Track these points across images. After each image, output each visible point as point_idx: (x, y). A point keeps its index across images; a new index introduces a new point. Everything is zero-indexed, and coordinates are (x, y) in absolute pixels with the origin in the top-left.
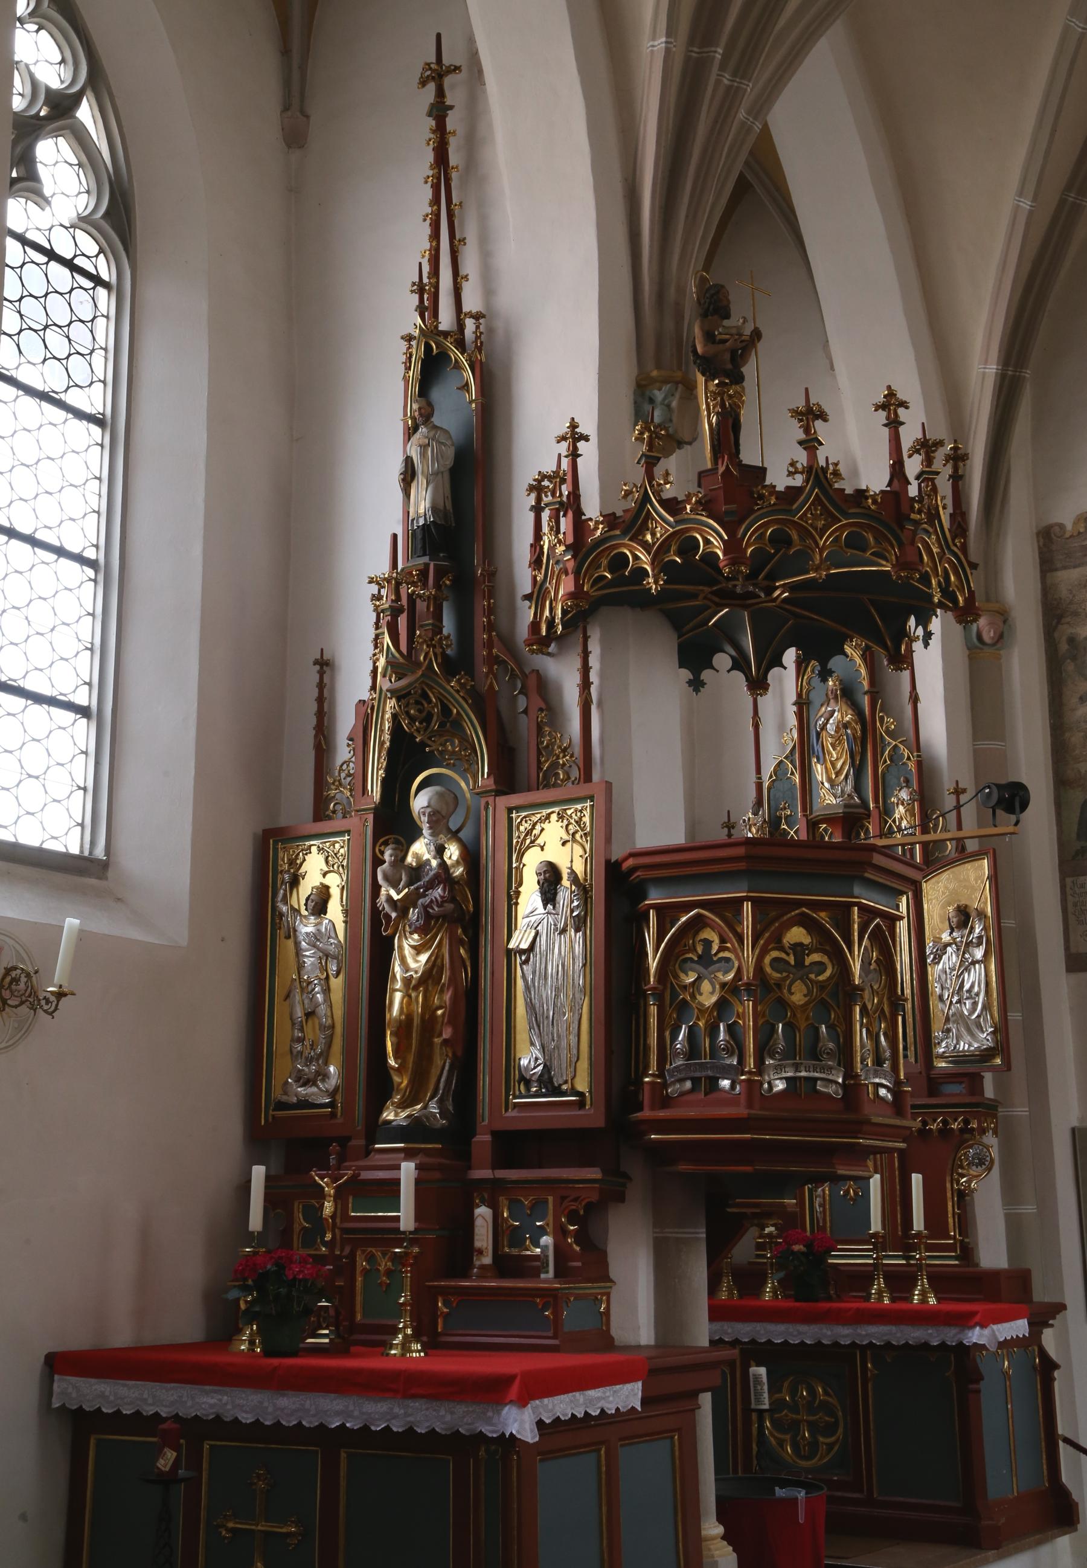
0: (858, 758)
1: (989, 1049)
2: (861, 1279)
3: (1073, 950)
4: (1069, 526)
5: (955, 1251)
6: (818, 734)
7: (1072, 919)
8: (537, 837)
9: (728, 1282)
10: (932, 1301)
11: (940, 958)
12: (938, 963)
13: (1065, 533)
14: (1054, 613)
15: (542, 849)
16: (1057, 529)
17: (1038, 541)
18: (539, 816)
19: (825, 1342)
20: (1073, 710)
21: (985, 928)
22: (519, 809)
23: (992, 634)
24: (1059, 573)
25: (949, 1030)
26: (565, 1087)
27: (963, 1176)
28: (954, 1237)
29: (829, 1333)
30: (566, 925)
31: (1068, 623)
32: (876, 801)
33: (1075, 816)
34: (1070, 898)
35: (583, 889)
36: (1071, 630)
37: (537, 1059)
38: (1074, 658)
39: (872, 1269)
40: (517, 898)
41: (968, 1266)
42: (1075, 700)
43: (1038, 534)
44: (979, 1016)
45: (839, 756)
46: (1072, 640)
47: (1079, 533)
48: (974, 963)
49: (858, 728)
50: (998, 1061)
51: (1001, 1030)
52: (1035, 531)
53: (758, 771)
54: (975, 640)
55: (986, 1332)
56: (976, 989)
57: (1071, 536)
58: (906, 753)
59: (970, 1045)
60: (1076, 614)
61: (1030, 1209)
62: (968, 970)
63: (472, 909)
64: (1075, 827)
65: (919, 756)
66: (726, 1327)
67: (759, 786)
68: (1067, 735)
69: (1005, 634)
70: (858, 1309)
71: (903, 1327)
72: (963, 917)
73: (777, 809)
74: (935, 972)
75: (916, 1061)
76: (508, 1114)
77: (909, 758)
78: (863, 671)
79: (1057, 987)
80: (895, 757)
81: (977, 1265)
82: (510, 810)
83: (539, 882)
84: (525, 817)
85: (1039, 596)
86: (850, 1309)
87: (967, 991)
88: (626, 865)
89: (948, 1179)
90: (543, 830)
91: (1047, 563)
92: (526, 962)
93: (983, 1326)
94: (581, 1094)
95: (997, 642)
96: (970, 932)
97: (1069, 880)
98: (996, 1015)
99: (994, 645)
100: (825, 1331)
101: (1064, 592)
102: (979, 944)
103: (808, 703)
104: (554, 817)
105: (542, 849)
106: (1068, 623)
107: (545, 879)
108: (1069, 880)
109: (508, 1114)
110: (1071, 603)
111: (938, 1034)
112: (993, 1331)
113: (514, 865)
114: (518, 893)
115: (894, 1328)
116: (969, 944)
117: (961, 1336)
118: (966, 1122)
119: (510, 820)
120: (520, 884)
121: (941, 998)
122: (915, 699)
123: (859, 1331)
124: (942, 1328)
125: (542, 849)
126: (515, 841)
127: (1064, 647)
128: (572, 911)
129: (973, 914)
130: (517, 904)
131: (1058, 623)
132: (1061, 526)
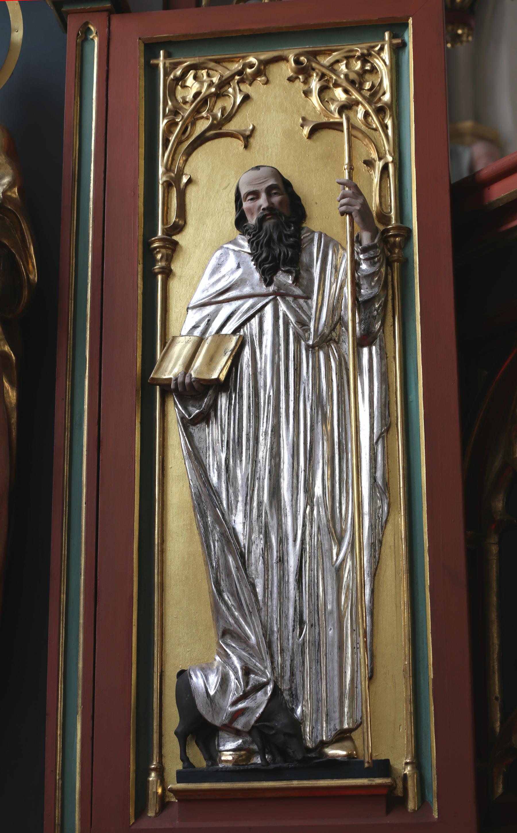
8: (228, 118)
15: (247, 139)
18: (236, 66)
22: (173, 46)
26: (336, 752)
30: (337, 322)
35: (384, 242)
37: (247, 671)
40: (169, 259)
63: (34, 277)
76: (143, 824)
82: (151, 49)
83: (241, 222)
84: (195, 67)
88: (500, 192)
90: (246, 98)
92: (206, 417)
94: (383, 767)
104: (287, 69)
105: (247, 139)
107: (271, 209)
109: (143, 824)
113: (162, 178)
114: (172, 248)
119: (151, 71)
120: (178, 228)
125: (246, 147)
126: (163, 124)
128: (356, 286)
130: (168, 273)
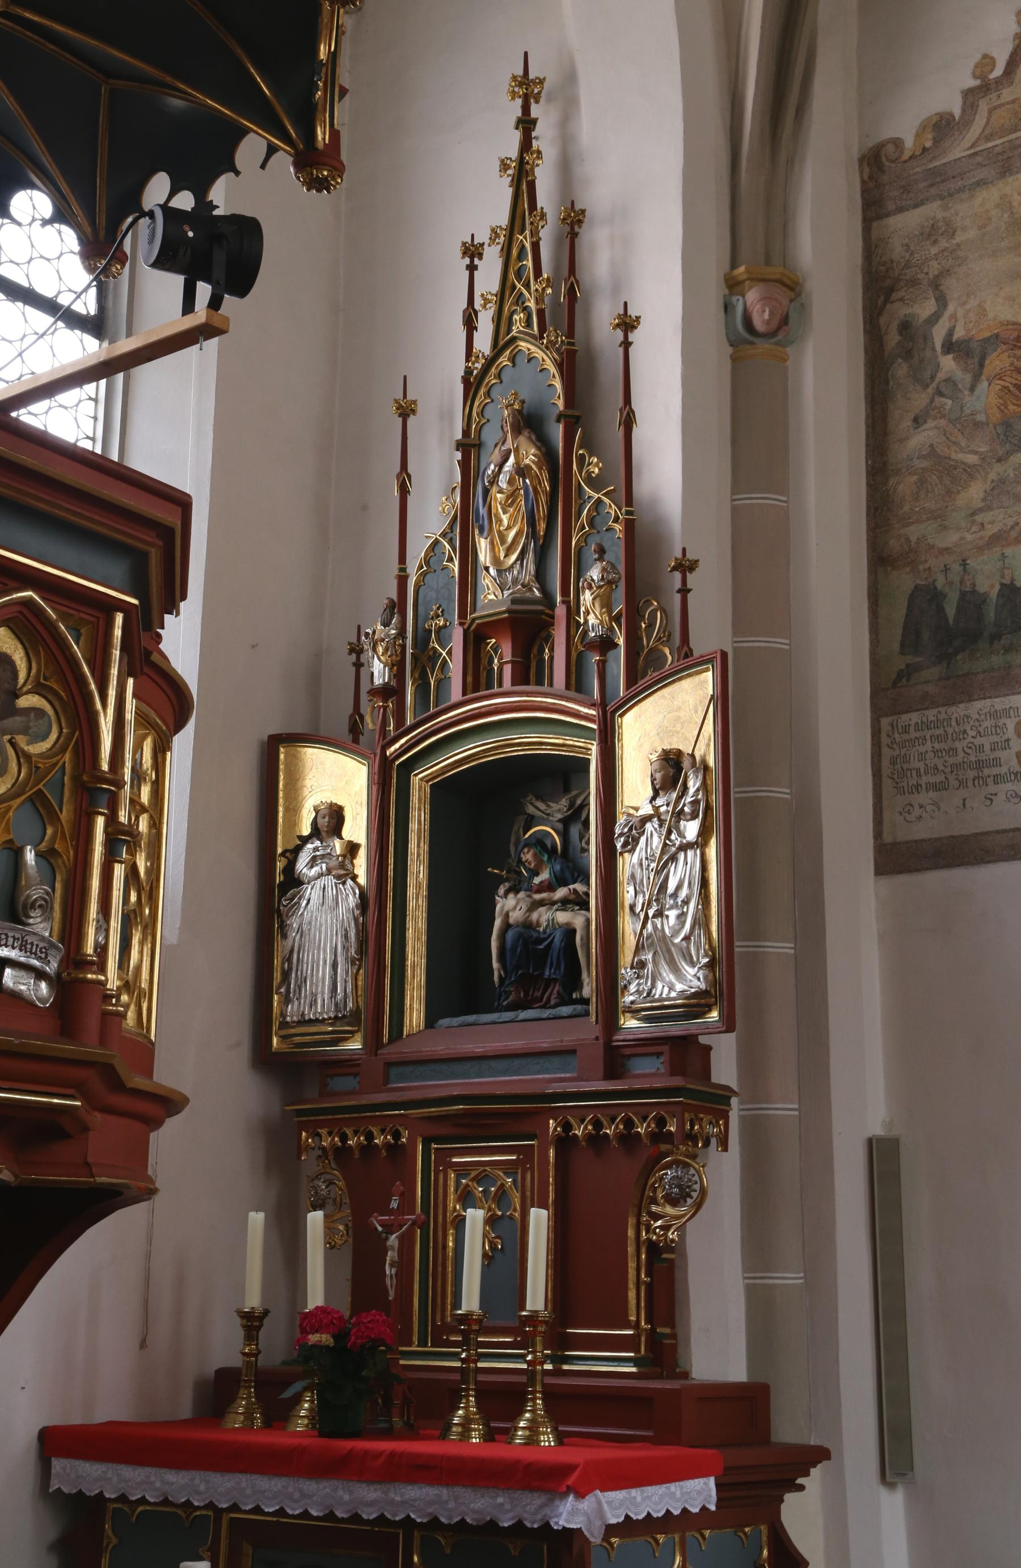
0: (542, 527)
1: (699, 994)
2: (441, 1396)
3: (887, 838)
4: (909, 142)
5: (637, 1350)
6: (486, 492)
7: (887, 783)
9: (249, 1397)
10: (547, 1440)
11: (636, 841)
12: (632, 851)
13: (902, 152)
14: (881, 283)
16: (890, 148)
17: (861, 172)
19: (340, 1514)
20: (902, 441)
21: (704, 786)
23: (766, 316)
24: (892, 221)
25: (642, 965)
27: (656, 1217)
28: (637, 1326)
29: (346, 1497)
31: (902, 299)
32: (565, 592)
33: (898, 612)
34: (885, 750)
36: (904, 311)
38: (908, 355)
39: (457, 1377)
41: (660, 1377)
42: (907, 423)
43: (861, 160)
44: (687, 938)
45: (509, 522)
46: (905, 327)
47: (925, 150)
48: (684, 847)
49: (545, 476)
50: (715, 1014)
51: (722, 964)
52: (856, 155)
53: (402, 558)
54: (740, 327)
55: (587, 1504)
56: (684, 893)
57: (912, 157)
58: (613, 510)
59: (671, 988)
60: (914, 283)
61: (791, 1278)
62: (674, 858)
64: (898, 632)
65: (628, 513)
66: (197, 1481)
67: (402, 580)
68: (892, 481)
69: (793, 316)
70: (393, 1454)
71: (459, 1490)
72: (671, 768)
73: (426, 620)
74: (627, 864)
75: (597, 1022)
77: (616, 520)
78: (558, 384)
79: (856, 901)
80: (598, 519)
81: (686, 1375)
85: (859, 260)
86: (379, 1455)
87: (671, 896)
89: (632, 1221)
91: (873, 207)
93: (581, 1495)
95: (779, 328)
96: (679, 798)
97: (885, 722)
98: (715, 935)
99: (773, 334)
100: (340, 1493)
101: (897, 250)
102: (694, 816)
103: (479, 446)
106: (902, 299)
108: (885, 722)
110: (908, 265)
111: (625, 972)
112: (599, 1503)
115: (444, 1492)
116: (679, 815)
117: (547, 1511)
118: (661, 1122)
121: (632, 907)
122: (628, 422)
123: (392, 1495)
124: (517, 1494)
127: (893, 339)
129: (686, 763)
131: (887, 300)
132: (898, 143)
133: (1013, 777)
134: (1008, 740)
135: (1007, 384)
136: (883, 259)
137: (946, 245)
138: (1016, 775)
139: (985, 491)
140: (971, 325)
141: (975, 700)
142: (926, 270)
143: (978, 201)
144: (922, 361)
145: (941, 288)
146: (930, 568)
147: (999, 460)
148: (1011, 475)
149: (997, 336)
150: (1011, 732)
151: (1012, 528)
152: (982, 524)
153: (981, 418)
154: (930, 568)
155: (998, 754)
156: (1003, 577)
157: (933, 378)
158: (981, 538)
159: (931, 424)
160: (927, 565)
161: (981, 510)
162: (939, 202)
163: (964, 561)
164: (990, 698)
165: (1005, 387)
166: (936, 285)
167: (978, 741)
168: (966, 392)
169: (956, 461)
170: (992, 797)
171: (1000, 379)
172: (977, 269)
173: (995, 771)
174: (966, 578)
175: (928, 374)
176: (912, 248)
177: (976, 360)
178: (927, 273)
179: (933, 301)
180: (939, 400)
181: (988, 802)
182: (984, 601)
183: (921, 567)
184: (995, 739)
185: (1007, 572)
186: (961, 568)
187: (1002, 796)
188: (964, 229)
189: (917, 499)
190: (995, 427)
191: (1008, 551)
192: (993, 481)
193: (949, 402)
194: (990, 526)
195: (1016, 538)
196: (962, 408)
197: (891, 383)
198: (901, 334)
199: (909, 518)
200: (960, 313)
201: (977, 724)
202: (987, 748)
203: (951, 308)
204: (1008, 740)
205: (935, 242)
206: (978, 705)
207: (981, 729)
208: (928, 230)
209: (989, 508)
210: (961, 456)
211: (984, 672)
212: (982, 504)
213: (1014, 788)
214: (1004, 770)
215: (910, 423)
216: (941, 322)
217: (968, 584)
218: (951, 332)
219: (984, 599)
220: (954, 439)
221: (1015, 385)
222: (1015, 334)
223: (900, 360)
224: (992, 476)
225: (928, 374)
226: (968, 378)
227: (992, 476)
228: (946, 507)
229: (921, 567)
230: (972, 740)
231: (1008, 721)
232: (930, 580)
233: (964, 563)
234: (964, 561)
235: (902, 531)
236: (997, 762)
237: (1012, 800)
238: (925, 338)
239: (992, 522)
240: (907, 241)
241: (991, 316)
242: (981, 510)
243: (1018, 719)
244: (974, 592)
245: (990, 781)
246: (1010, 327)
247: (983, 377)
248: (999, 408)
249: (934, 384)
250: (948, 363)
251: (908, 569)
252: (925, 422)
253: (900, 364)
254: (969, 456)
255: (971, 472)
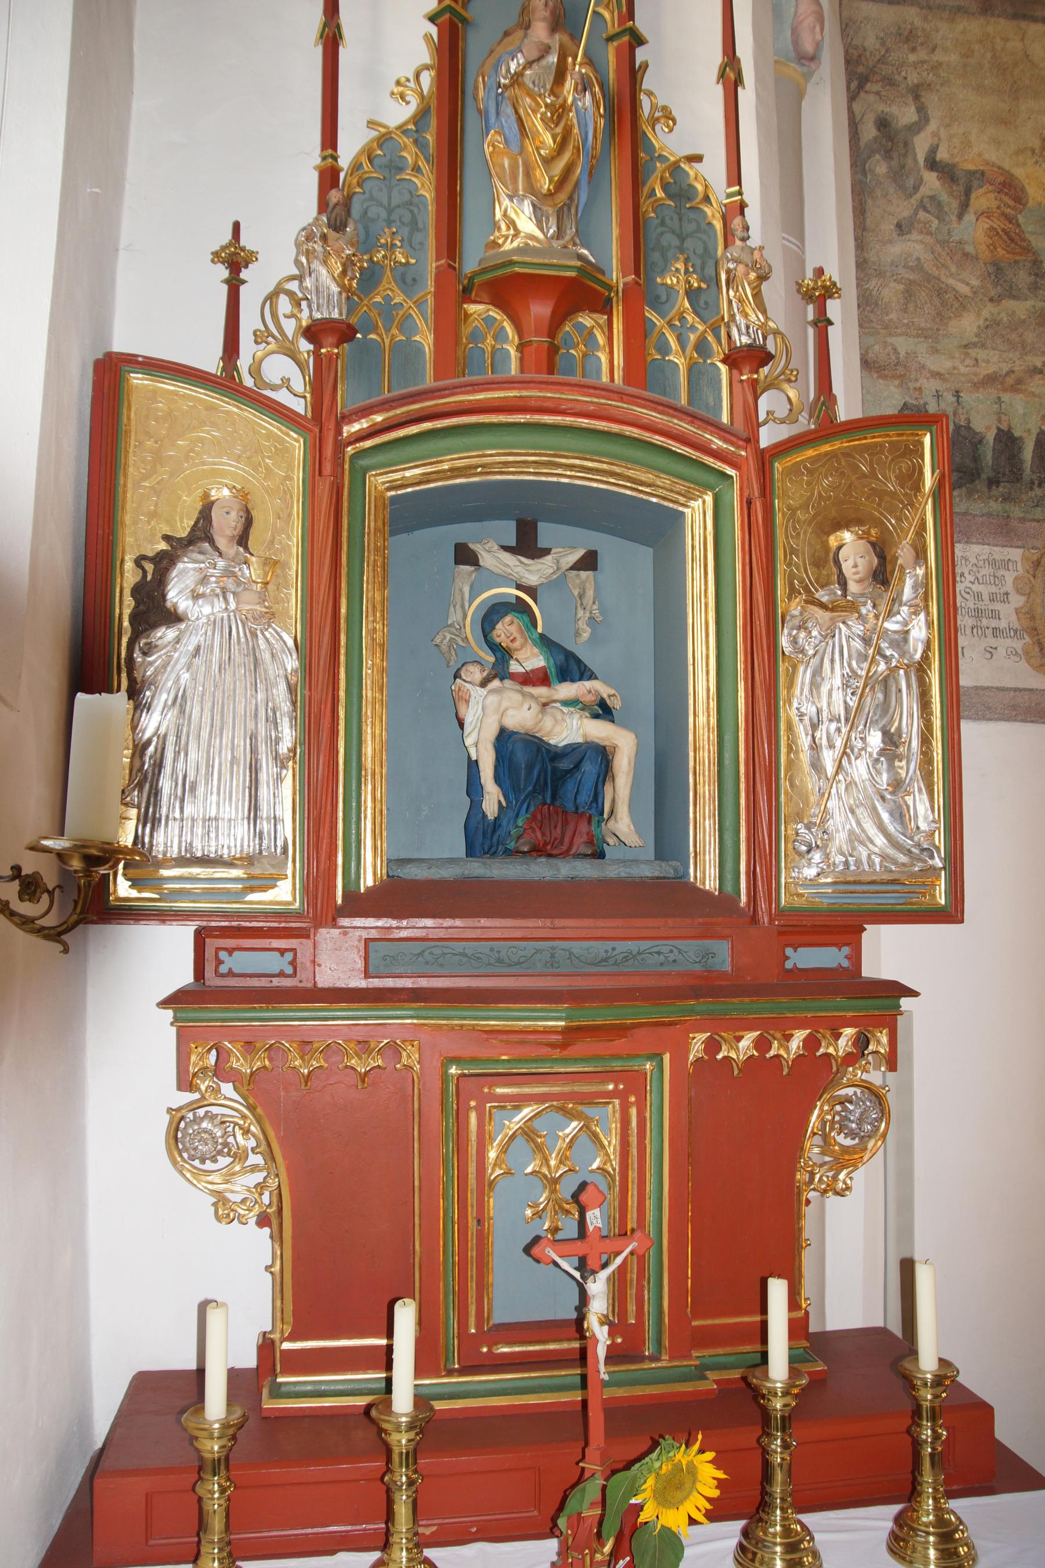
42: (888, 227)
46: (883, 124)
60: (889, 82)
106: (878, 93)
133: (1012, 634)
134: (1007, 594)
135: (995, 226)
136: (854, 42)
137: (926, 58)
138: (1016, 631)
139: (979, 327)
140: (955, 151)
141: (972, 543)
142: (903, 74)
143: (960, 28)
144: (903, 167)
145: (923, 100)
146: (920, 388)
147: (991, 300)
148: (1005, 319)
149: (983, 173)
150: (1009, 586)
151: (1007, 374)
152: (976, 360)
153: (969, 249)
154: (920, 388)
155: (998, 606)
156: (999, 421)
157: (916, 188)
158: (975, 374)
159: (915, 236)
160: (918, 385)
161: (975, 345)
162: (918, 10)
163: (957, 392)
164: (989, 544)
165: (995, 229)
166: (916, 93)
167: (976, 587)
168: (954, 218)
169: (947, 285)
170: (993, 651)
171: (988, 217)
172: (961, 96)
173: (994, 623)
174: (960, 411)
175: (910, 182)
176: (888, 43)
177: (962, 188)
178: (905, 78)
179: (913, 109)
180: (922, 215)
181: (988, 655)
182: (980, 442)
183: (911, 385)
184: (993, 589)
185: (1004, 418)
186: (954, 399)
187: (1001, 652)
188: (945, 50)
189: (905, 310)
190: (985, 264)
191: (1006, 397)
192: (986, 320)
193: (937, 222)
194: (984, 364)
195: (1012, 386)
196: (949, 233)
197: (869, 177)
198: (879, 130)
199: (897, 328)
200: (943, 133)
201: (975, 569)
202: (985, 597)
203: (933, 126)
204: (1007, 594)
205: (913, 50)
206: (976, 548)
207: (979, 576)
208: (906, 34)
209: (983, 346)
210: (951, 281)
211: (982, 515)
212: (976, 339)
213: (1014, 645)
214: (1003, 624)
215: (892, 227)
216: (922, 135)
217: (963, 418)
218: (933, 150)
219: (977, 441)
220: (942, 261)
221: (1003, 230)
222: (1001, 179)
223: (878, 156)
224: (985, 313)
225: (910, 182)
226: (955, 204)
227: (985, 313)
228: (938, 330)
229: (911, 385)
230: (970, 585)
231: (1006, 573)
232: (922, 402)
233: (957, 394)
234: (957, 392)
235: (890, 340)
236: (995, 615)
237: (1012, 657)
238: (906, 144)
239: (988, 362)
240: (882, 35)
241: (975, 150)
242: (975, 345)
243: (1015, 574)
244: (968, 428)
245: (989, 632)
246: (996, 169)
247: (971, 209)
248: (988, 246)
249: (918, 196)
250: (932, 181)
251: (897, 382)
252: (909, 232)
253: (878, 161)
254: (960, 284)
255: (962, 304)
